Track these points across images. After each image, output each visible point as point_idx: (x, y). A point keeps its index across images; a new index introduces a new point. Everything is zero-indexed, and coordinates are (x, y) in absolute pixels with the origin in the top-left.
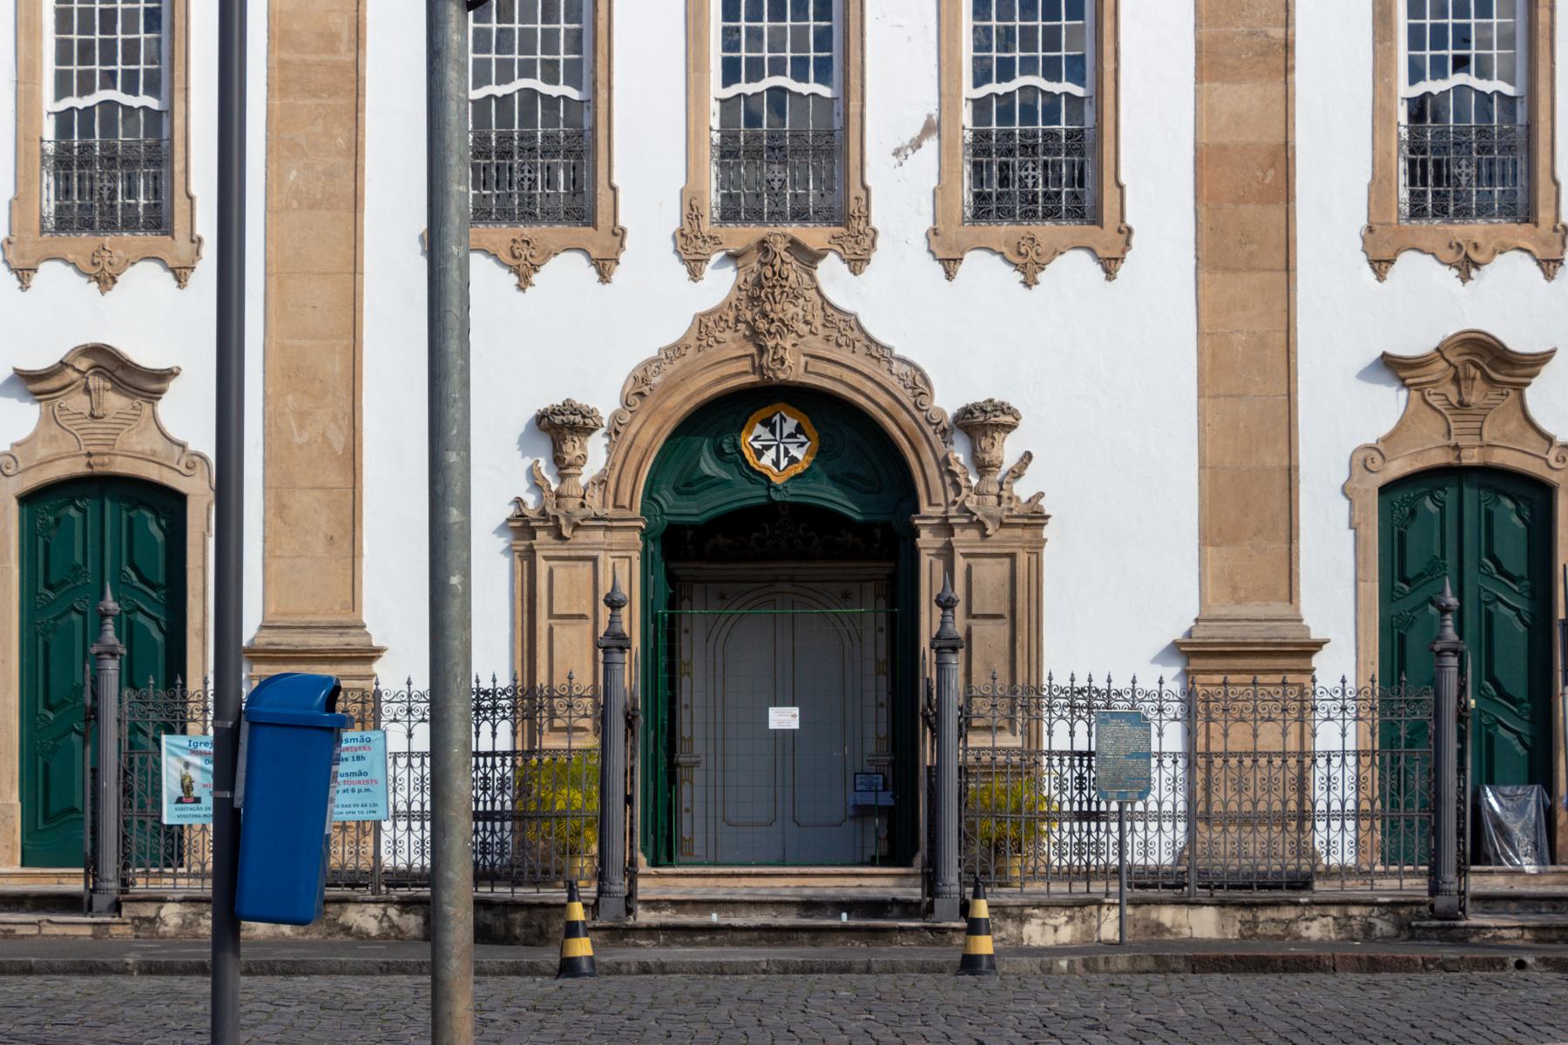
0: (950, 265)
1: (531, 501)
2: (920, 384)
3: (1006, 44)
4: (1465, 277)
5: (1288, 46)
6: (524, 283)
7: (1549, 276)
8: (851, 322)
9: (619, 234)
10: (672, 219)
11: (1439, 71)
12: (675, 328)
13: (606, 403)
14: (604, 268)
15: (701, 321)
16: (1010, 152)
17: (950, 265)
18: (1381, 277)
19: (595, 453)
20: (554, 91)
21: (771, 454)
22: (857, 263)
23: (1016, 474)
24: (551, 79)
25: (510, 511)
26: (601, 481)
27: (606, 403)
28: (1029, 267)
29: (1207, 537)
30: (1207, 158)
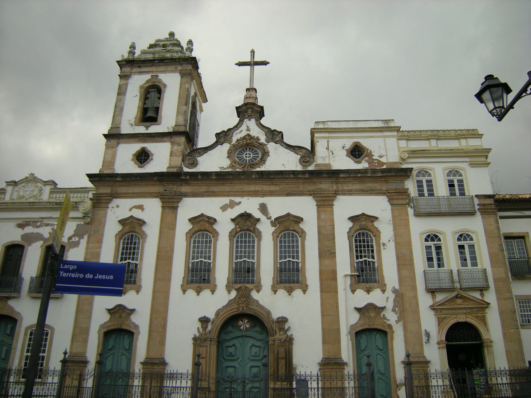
1: (197, 334)
2: (269, 313)
4: (368, 293)
5: (335, 253)
6: (198, 294)
7: (384, 293)
8: (257, 301)
10: (225, 282)
11: (361, 257)
12: (225, 303)
13: (211, 315)
14: (213, 292)
15: (230, 301)
16: (286, 271)
18: (353, 294)
19: (210, 327)
20: (206, 261)
21: (243, 326)
22: (258, 291)
23: (287, 330)
24: (205, 259)
25: (193, 336)
27: (211, 315)
28: (290, 291)
29: (324, 343)
30: (321, 272)
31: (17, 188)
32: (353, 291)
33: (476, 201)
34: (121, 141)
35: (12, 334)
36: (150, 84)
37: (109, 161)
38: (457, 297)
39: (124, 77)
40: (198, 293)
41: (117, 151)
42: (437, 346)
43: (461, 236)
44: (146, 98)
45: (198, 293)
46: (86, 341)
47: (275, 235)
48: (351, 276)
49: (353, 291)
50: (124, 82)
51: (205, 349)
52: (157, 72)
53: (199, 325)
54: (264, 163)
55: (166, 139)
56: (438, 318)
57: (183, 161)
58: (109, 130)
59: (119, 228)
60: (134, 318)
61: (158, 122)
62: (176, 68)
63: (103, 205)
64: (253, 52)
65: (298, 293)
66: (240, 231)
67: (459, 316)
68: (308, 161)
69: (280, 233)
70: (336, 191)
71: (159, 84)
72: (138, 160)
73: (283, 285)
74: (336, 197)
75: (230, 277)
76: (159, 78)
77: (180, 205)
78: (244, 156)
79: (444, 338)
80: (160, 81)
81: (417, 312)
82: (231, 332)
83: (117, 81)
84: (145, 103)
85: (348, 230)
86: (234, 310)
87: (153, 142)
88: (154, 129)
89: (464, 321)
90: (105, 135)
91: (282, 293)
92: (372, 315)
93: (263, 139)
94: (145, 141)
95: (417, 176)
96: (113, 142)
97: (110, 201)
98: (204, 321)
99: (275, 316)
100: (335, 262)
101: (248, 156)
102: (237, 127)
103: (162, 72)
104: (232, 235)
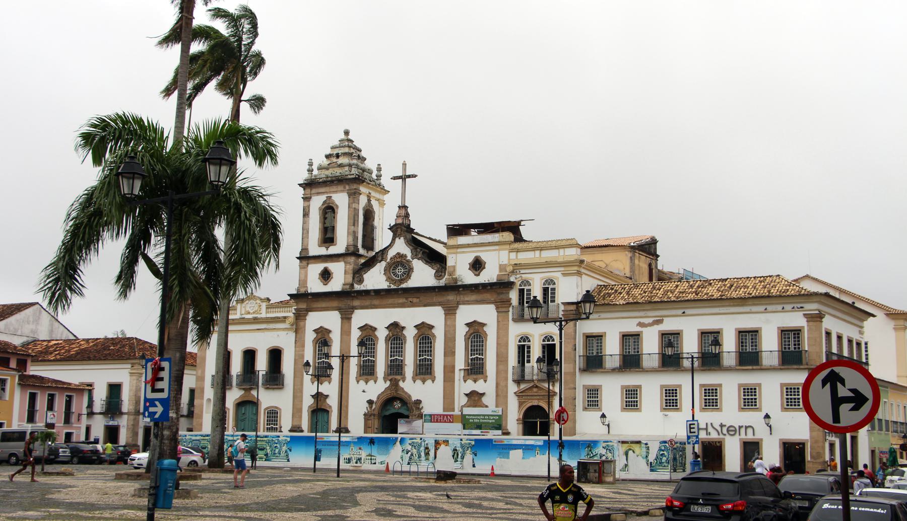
0: (414, 382)
2: (410, 396)
3: (423, 352)
5: (455, 352)
6: (366, 384)
8: (403, 389)
9: (377, 377)
10: (383, 375)
13: (375, 399)
14: (375, 382)
17: (414, 382)
22: (404, 381)
26: (374, 410)
27: (375, 399)
28: (424, 382)
30: (445, 367)
31: (243, 305)
32: (465, 381)
33: (562, 307)
34: (310, 261)
35: (257, 414)
36: (326, 205)
37: (303, 282)
38: (533, 387)
39: (306, 199)
40: (367, 383)
41: (307, 270)
42: (516, 422)
43: (546, 337)
44: (325, 218)
45: (367, 383)
46: (301, 417)
47: (416, 339)
48: (465, 370)
49: (465, 381)
50: (307, 203)
51: (370, 421)
52: (330, 192)
53: (367, 405)
54: (410, 278)
55: (341, 259)
56: (519, 402)
57: (353, 278)
58: (300, 253)
59: (315, 335)
60: (328, 401)
61: (335, 243)
62: (345, 188)
63: (302, 318)
64: (404, 165)
65: (429, 382)
66: (393, 336)
67: (534, 401)
68: (441, 275)
69: (419, 337)
70: (458, 302)
71: (333, 205)
72: (322, 277)
73: (419, 377)
74: (458, 307)
75: (386, 371)
76: (332, 198)
77: (353, 316)
78: (397, 271)
79: (521, 417)
80: (333, 202)
81: (506, 397)
82: (389, 409)
83: (301, 203)
84: (325, 223)
85: (465, 333)
86: (389, 395)
87: (332, 261)
88: (333, 250)
89: (536, 404)
90: (298, 258)
91: (419, 382)
92: (476, 399)
93: (409, 257)
94: (326, 261)
95: (520, 285)
96: (305, 263)
97: (306, 315)
98: (370, 402)
99: (414, 398)
100: (455, 359)
101: (400, 271)
102: (390, 246)
103: (336, 192)
104: (387, 339)
